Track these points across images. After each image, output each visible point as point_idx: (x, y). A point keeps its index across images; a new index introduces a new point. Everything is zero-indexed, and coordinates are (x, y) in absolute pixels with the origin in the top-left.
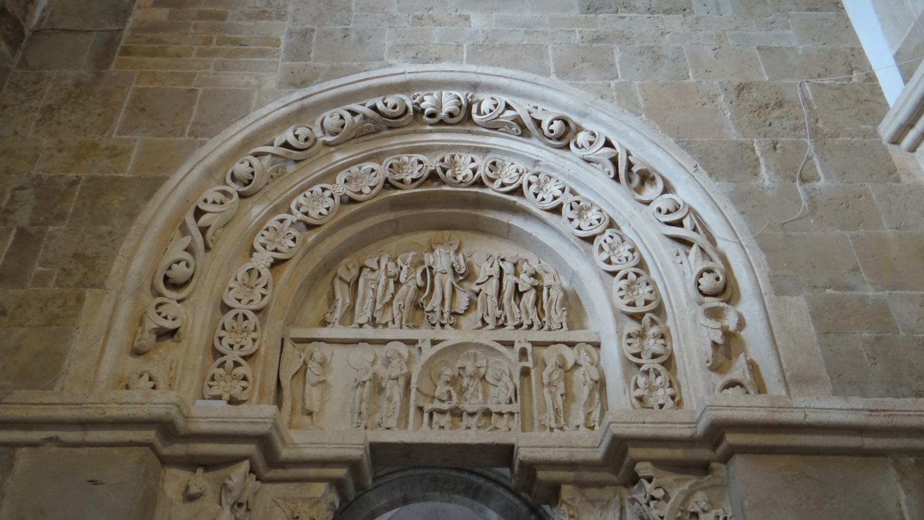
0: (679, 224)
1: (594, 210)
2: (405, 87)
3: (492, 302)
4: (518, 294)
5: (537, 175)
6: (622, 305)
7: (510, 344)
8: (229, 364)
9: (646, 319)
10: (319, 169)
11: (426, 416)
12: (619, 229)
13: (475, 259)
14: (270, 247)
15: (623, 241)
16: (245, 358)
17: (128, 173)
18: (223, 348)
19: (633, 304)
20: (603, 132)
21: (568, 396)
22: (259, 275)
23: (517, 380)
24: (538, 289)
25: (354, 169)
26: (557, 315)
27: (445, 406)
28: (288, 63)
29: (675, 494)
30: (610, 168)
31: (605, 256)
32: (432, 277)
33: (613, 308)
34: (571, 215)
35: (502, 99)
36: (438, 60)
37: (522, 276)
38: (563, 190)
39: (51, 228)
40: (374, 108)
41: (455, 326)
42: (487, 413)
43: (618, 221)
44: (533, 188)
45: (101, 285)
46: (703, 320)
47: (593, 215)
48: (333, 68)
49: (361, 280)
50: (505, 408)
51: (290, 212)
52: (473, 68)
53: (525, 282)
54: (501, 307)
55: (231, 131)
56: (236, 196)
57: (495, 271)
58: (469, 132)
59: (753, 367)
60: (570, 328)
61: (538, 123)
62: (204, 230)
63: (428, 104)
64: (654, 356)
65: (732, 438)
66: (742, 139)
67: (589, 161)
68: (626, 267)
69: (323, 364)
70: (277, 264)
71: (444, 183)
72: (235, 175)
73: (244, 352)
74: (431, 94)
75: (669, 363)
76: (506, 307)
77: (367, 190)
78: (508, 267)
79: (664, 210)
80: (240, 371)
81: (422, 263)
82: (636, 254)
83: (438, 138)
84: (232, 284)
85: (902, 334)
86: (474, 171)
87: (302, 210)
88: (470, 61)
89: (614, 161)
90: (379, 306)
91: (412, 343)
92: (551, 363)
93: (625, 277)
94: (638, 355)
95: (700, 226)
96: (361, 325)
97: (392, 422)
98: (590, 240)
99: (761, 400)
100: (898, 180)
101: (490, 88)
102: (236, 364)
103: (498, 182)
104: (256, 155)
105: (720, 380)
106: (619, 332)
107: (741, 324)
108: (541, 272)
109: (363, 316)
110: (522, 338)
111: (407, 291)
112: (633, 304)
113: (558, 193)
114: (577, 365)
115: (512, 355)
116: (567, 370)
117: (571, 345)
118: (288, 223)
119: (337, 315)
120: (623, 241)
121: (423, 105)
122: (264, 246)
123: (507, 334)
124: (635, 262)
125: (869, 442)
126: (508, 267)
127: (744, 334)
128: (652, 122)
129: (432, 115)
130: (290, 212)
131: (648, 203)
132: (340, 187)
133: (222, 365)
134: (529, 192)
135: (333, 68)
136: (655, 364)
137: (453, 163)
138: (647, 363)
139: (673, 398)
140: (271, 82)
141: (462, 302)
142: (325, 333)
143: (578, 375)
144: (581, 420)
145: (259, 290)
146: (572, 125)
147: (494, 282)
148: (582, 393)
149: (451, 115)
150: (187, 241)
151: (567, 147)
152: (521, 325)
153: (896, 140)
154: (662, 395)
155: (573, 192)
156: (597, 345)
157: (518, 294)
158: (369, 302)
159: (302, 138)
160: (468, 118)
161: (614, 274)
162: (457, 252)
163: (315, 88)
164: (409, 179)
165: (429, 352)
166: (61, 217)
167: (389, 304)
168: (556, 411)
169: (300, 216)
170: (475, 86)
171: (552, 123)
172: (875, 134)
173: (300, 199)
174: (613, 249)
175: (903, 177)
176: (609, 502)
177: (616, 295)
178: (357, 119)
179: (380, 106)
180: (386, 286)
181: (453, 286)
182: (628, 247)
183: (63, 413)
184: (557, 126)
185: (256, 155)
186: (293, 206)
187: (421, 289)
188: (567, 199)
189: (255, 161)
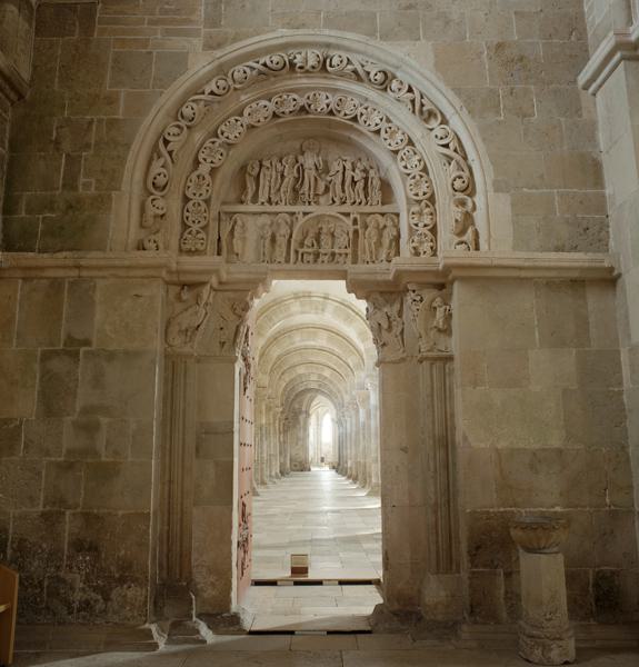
0: (446, 146)
1: (400, 132)
2: (284, 47)
3: (338, 187)
4: (354, 182)
5: (366, 109)
6: (411, 194)
7: (348, 215)
8: (194, 232)
9: (423, 204)
10: (233, 107)
11: (300, 256)
12: (413, 145)
13: (330, 158)
14: (209, 160)
15: (415, 154)
16: (202, 228)
17: (121, 117)
18: (190, 223)
19: (417, 195)
20: (407, 80)
21: (379, 244)
22: (204, 178)
23: (351, 236)
24: (366, 179)
25: (254, 105)
26: (376, 195)
27: (310, 250)
28: (207, 30)
29: (426, 300)
30: (410, 106)
31: (403, 163)
32: (303, 171)
33: (408, 198)
34: (386, 136)
35: (345, 55)
36: (304, 26)
37: (357, 171)
38: (381, 120)
39: (84, 154)
40: (265, 65)
41: (317, 203)
42: (333, 254)
43: (414, 140)
44: (364, 117)
45: (119, 189)
46: (453, 207)
47: (399, 136)
48: (237, 34)
49: (262, 175)
50: (343, 251)
51: (217, 137)
52: (327, 32)
53: (358, 175)
54: (344, 191)
55: (177, 83)
56: (185, 128)
57: (341, 169)
58: (325, 77)
59: (476, 234)
60: (383, 204)
61: (368, 73)
62: (170, 153)
63: (299, 61)
64: (425, 226)
65: (455, 273)
66: (492, 87)
67: (399, 101)
68: (416, 172)
69: (243, 226)
70: (213, 171)
71: (308, 113)
72: (184, 113)
73: (202, 224)
74: (300, 53)
75: (434, 230)
76: (347, 192)
77: (262, 120)
78: (348, 166)
79: (439, 136)
80: (199, 236)
81: (297, 162)
82: (422, 163)
83: (304, 82)
84: (189, 184)
85: (558, 214)
86: (328, 106)
87: (226, 134)
88: (325, 26)
89: (413, 101)
90: (272, 191)
91: (293, 214)
92: (372, 225)
93: (414, 178)
94: (416, 225)
95: (461, 149)
96: (263, 203)
97: (283, 260)
98: (396, 152)
99: (473, 252)
100: (580, 116)
101: (338, 47)
102: (198, 232)
103: (343, 113)
104: (193, 101)
105: (457, 239)
106: (409, 210)
107: (474, 208)
108: (368, 168)
109: (263, 198)
110: (354, 211)
111: (289, 180)
112: (417, 195)
113: (378, 121)
114: (385, 227)
115: (349, 222)
116: (381, 230)
117: (383, 214)
118: (217, 144)
119: (249, 197)
120: (415, 154)
122: (205, 160)
123: (345, 208)
124: (421, 167)
125: (523, 274)
126: (348, 166)
127: (474, 214)
128: (439, 74)
129: (301, 68)
130: (217, 137)
131: (431, 130)
132: (246, 120)
133: (190, 233)
134: (361, 120)
135: (237, 34)
136: (425, 230)
137: (315, 100)
138: (421, 230)
139: (432, 248)
140: (198, 43)
141: (321, 188)
142: (242, 208)
143: (385, 232)
144: (384, 257)
145: (205, 187)
146: (389, 75)
147: (340, 176)
148: (386, 242)
149: (313, 67)
150: (162, 161)
151: (385, 89)
152: (354, 203)
153: (586, 87)
154: (426, 246)
155: (388, 121)
156: (398, 215)
157: (354, 182)
158: (267, 188)
159: (221, 87)
160: (324, 68)
161: (409, 175)
162: (318, 156)
163: (229, 49)
164: (287, 111)
165: (302, 220)
166: (88, 146)
167: (279, 190)
168: (371, 252)
169: (223, 139)
170: (328, 46)
172: (575, 81)
173: (223, 127)
174: (408, 159)
175: (585, 115)
176: (395, 300)
177: (408, 188)
178: (254, 72)
179: (268, 63)
180: (277, 178)
181: (316, 179)
182: (417, 157)
183: (117, 263)
184: (380, 77)
185: (193, 101)
186: (219, 132)
187: (297, 180)
188: (384, 125)
189: (194, 106)
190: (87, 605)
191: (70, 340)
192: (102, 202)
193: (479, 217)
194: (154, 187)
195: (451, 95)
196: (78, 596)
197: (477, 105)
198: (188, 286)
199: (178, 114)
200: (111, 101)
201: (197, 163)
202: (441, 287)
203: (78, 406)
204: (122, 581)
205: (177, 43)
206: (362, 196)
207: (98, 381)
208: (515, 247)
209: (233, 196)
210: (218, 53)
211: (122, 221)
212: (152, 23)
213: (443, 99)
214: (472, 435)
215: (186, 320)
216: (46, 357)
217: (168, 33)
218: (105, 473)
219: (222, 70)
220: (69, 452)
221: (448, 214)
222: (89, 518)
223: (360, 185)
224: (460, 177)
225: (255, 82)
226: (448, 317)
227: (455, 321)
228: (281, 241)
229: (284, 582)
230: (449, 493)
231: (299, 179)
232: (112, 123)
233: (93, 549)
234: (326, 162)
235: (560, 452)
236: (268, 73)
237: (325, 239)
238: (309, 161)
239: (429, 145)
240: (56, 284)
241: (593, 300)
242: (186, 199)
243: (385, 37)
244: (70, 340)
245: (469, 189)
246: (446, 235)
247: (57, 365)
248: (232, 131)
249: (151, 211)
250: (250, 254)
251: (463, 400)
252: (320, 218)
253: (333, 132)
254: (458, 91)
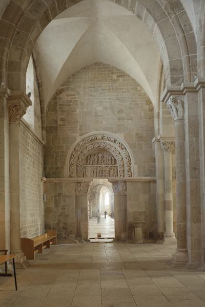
21: (114, 173)
53: (110, 159)
63: (98, 138)
75: (124, 171)
109: (91, 163)
115: (108, 168)
132: (88, 149)
140: (78, 134)
166: (58, 157)
190: (65, 237)
191: (59, 193)
192: (62, 167)
193: (132, 168)
194: (71, 165)
196: (64, 236)
197: (133, 146)
198: (79, 183)
199: (75, 149)
200: (62, 147)
201: (79, 158)
202: (125, 182)
203: (61, 205)
204: (71, 234)
205: (74, 135)
207: (64, 201)
208: (138, 176)
209: (85, 163)
211: (66, 171)
212: (69, 130)
213: (126, 145)
214: (130, 210)
215: (79, 189)
216: (55, 196)
217: (72, 132)
218: (67, 216)
219: (83, 140)
220: (61, 213)
221: (126, 168)
222: (65, 224)
223: (110, 161)
226: (126, 188)
227: (127, 189)
228: (95, 172)
229: (96, 238)
230: (126, 219)
231: (98, 159)
232: (63, 152)
233: (66, 229)
234: (103, 155)
235: (145, 212)
236: (91, 140)
238: (100, 155)
239: (123, 153)
240: (56, 184)
241: (152, 184)
242: (77, 166)
243: (115, 133)
244: (59, 193)
245: (130, 164)
246: (126, 172)
247: (57, 198)
248: (85, 152)
249: (71, 169)
250: (89, 175)
251: (128, 203)
253: (104, 150)
254: (128, 144)
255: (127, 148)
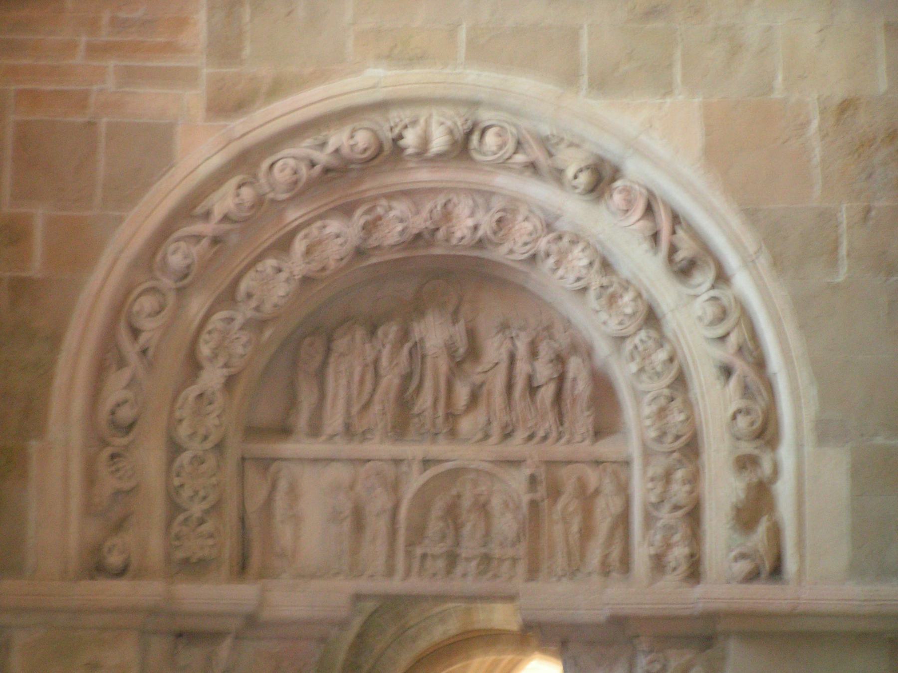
3: (498, 399)
24: (561, 379)
63: (411, 139)
70: (230, 382)
91: (397, 462)
109: (334, 421)
121: (402, 143)
123: (516, 446)
171: (576, 177)
180: (362, 382)
195: (736, 222)
206: (551, 418)
210: (238, 125)
223: (547, 393)
224: (748, 412)
225: (312, 184)
228: (378, 525)
237: (471, 525)
252: (456, 473)
254: (751, 215)
255: (732, 260)
